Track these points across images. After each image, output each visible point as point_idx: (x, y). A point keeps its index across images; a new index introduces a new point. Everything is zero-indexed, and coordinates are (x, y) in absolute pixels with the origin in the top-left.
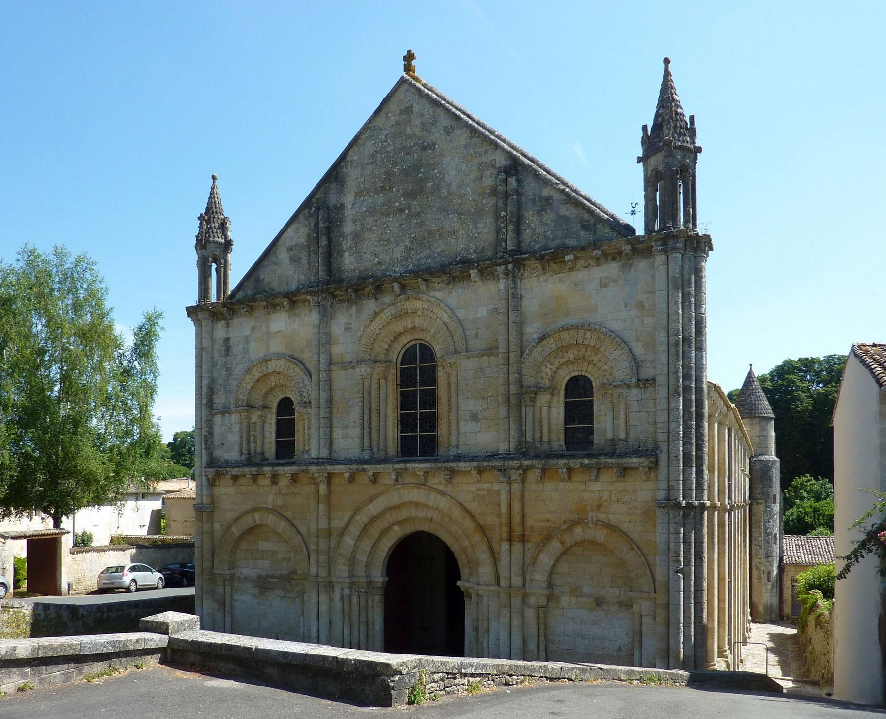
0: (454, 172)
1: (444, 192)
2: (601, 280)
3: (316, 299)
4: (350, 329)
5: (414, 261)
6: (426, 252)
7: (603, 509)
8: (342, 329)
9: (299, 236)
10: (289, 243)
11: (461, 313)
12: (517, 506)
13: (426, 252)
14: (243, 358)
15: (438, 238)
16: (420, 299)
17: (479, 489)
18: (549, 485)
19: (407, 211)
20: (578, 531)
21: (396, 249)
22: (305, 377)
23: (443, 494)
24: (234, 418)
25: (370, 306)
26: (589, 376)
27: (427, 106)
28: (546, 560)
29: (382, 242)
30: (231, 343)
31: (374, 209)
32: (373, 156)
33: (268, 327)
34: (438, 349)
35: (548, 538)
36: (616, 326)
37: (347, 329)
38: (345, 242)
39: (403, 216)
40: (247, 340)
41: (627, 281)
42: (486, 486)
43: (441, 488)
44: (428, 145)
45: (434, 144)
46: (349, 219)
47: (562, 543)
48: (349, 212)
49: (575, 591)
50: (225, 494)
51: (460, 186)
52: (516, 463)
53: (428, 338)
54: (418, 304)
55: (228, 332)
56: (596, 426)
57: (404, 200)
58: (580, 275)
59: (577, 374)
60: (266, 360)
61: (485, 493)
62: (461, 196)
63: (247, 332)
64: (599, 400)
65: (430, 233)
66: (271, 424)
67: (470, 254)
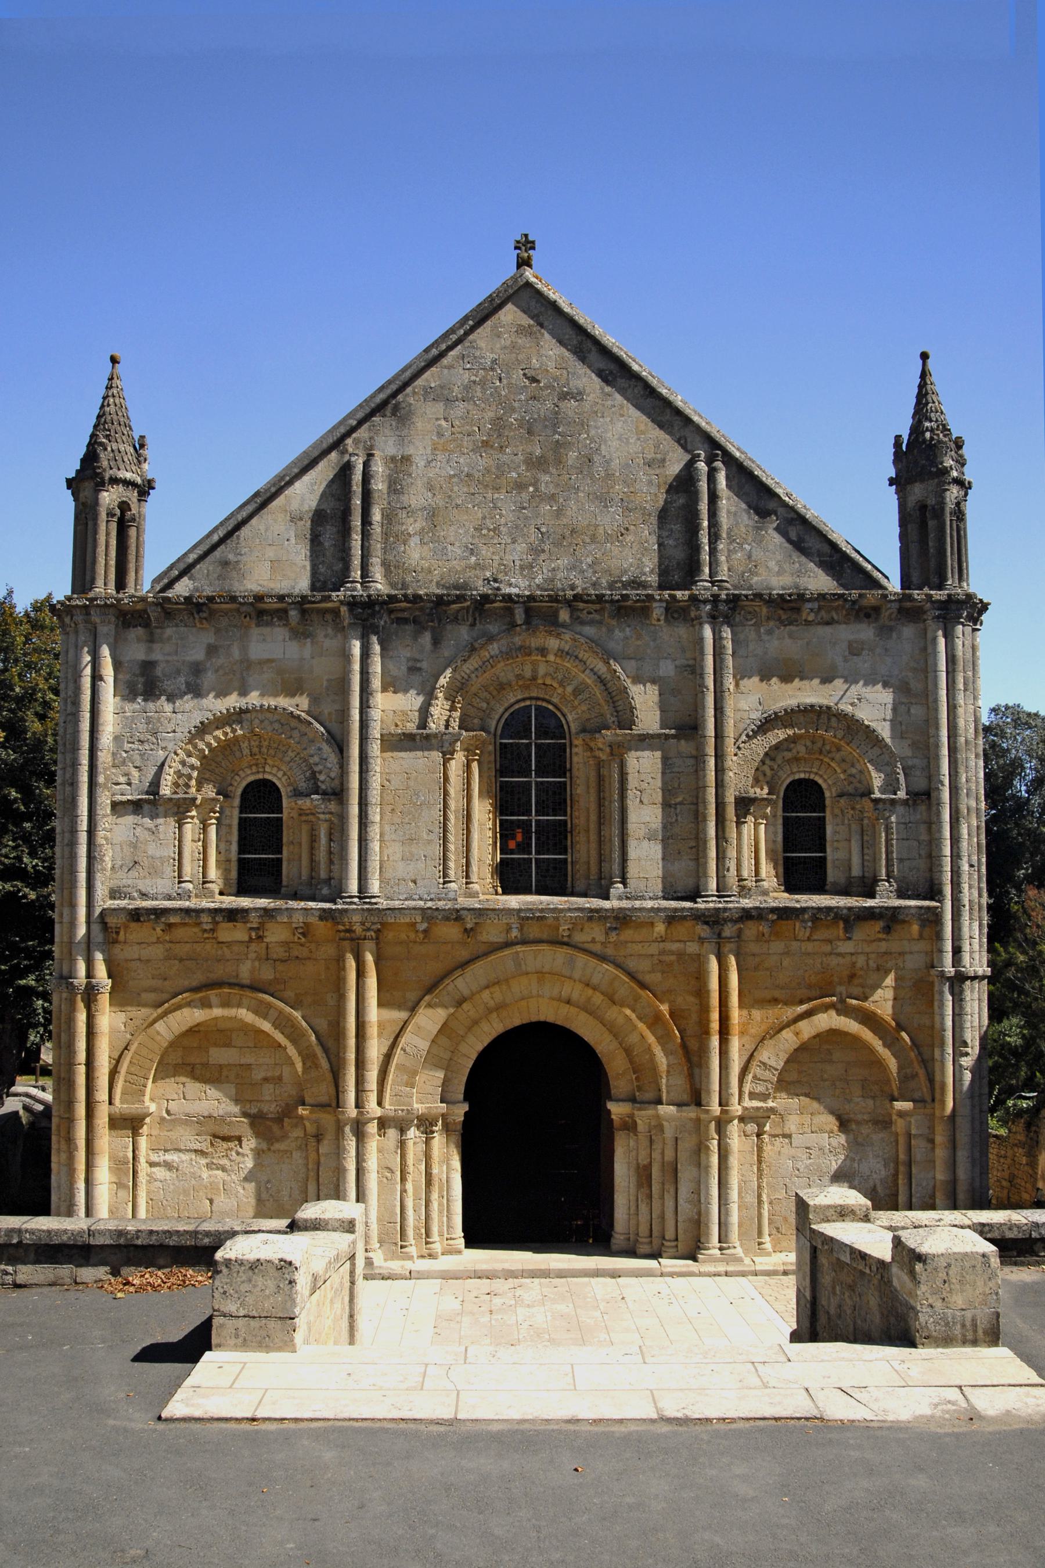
1: (599, 470)
2: (850, 644)
4: (420, 669)
5: (545, 571)
7: (856, 981)
8: (404, 668)
10: (295, 505)
15: (588, 540)
17: (663, 952)
19: (531, 489)
21: (512, 546)
26: (820, 781)
29: (484, 532)
30: (159, 671)
33: (244, 649)
34: (572, 719)
38: (412, 519)
39: (523, 495)
41: (886, 650)
42: (675, 946)
44: (568, 393)
47: (797, 1034)
50: (139, 959)
54: (553, 643)
55: (150, 650)
56: (830, 854)
57: (527, 470)
59: (802, 776)
64: (835, 816)
65: (573, 531)
66: (230, 826)
67: (645, 574)
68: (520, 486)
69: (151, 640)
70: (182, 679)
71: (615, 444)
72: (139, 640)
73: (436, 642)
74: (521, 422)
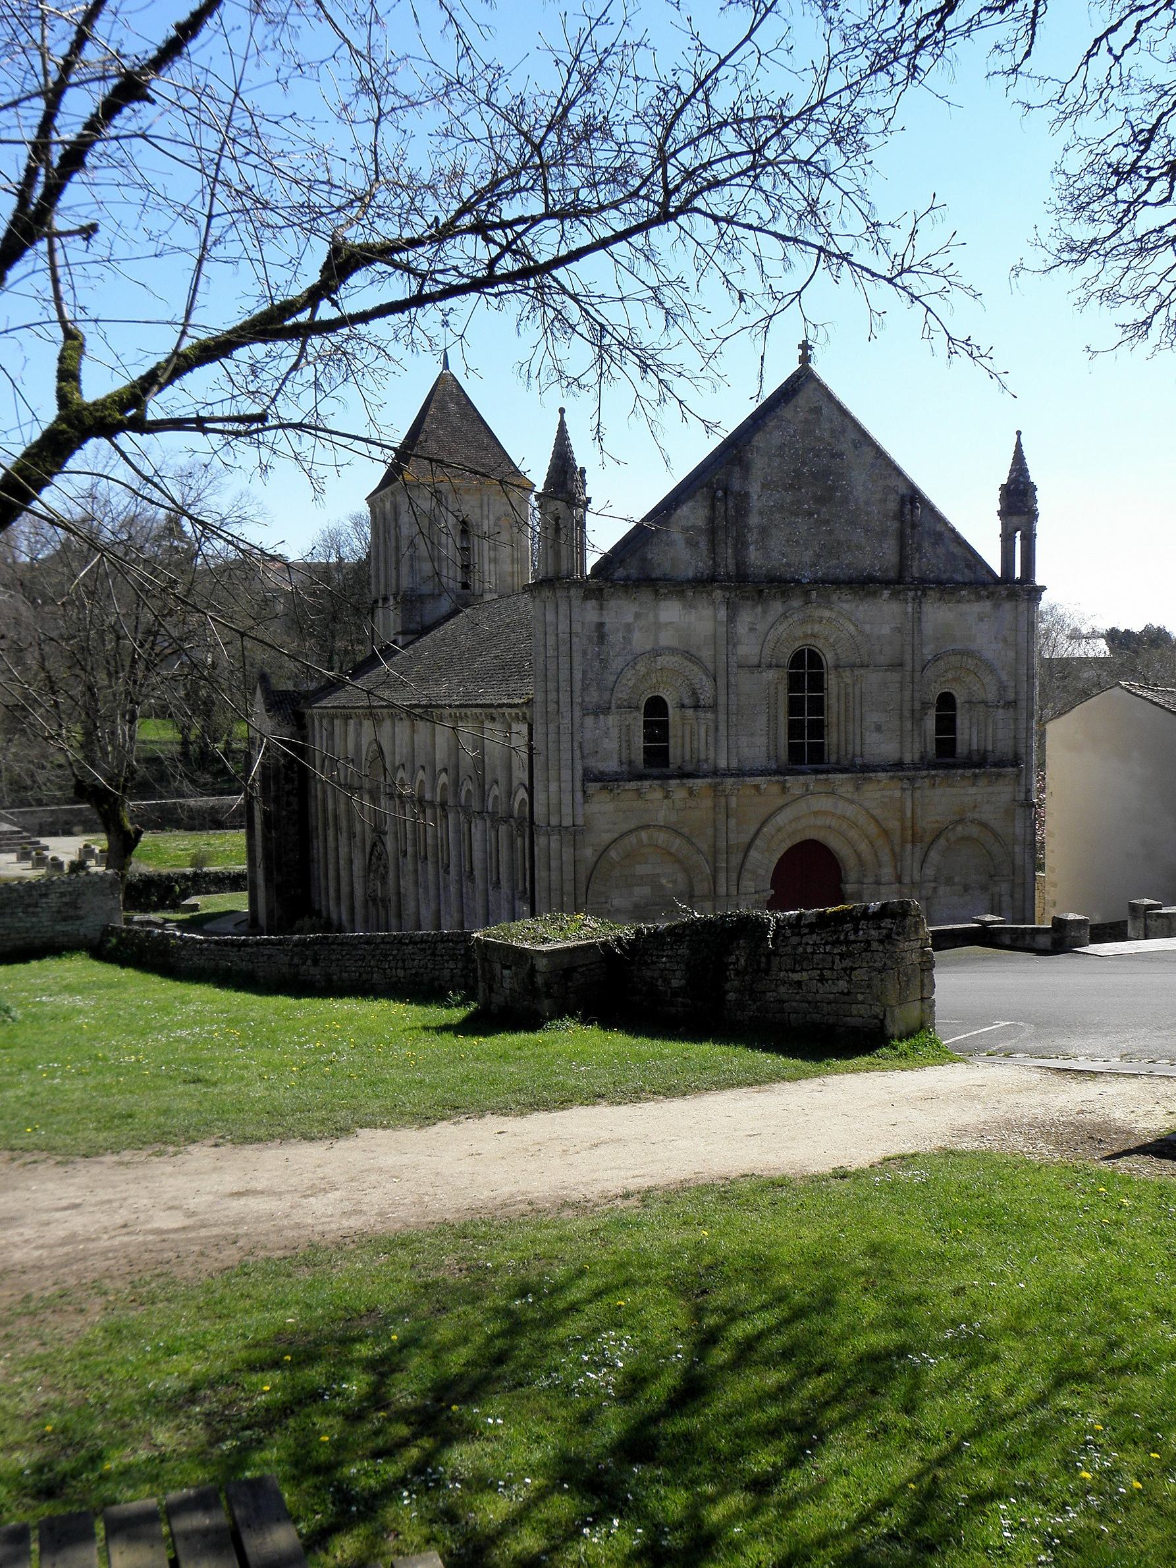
0: (861, 488)
1: (852, 506)
3: (727, 594)
6: (834, 562)
9: (693, 514)
11: (867, 628)
12: (918, 810)
13: (834, 562)
14: (624, 649)
16: (831, 609)
17: (883, 796)
18: (938, 791)
20: (959, 828)
22: (704, 678)
23: (852, 802)
24: (612, 720)
25: (777, 607)
27: (836, 412)
28: (934, 856)
31: (782, 506)
32: (780, 447)
33: (656, 616)
34: (828, 658)
35: (938, 836)
36: (989, 655)
37: (752, 629)
40: (629, 628)
43: (849, 796)
45: (843, 454)
46: (755, 510)
48: (755, 503)
49: (949, 881)
51: (867, 503)
52: (925, 773)
53: (819, 645)
54: (827, 614)
58: (965, 607)
60: (656, 653)
61: (886, 800)
62: (868, 514)
63: (630, 619)
68: (811, 514)
69: (601, 608)
70: (621, 635)
71: (861, 488)
72: (593, 608)
73: (764, 612)
74: (811, 473)
